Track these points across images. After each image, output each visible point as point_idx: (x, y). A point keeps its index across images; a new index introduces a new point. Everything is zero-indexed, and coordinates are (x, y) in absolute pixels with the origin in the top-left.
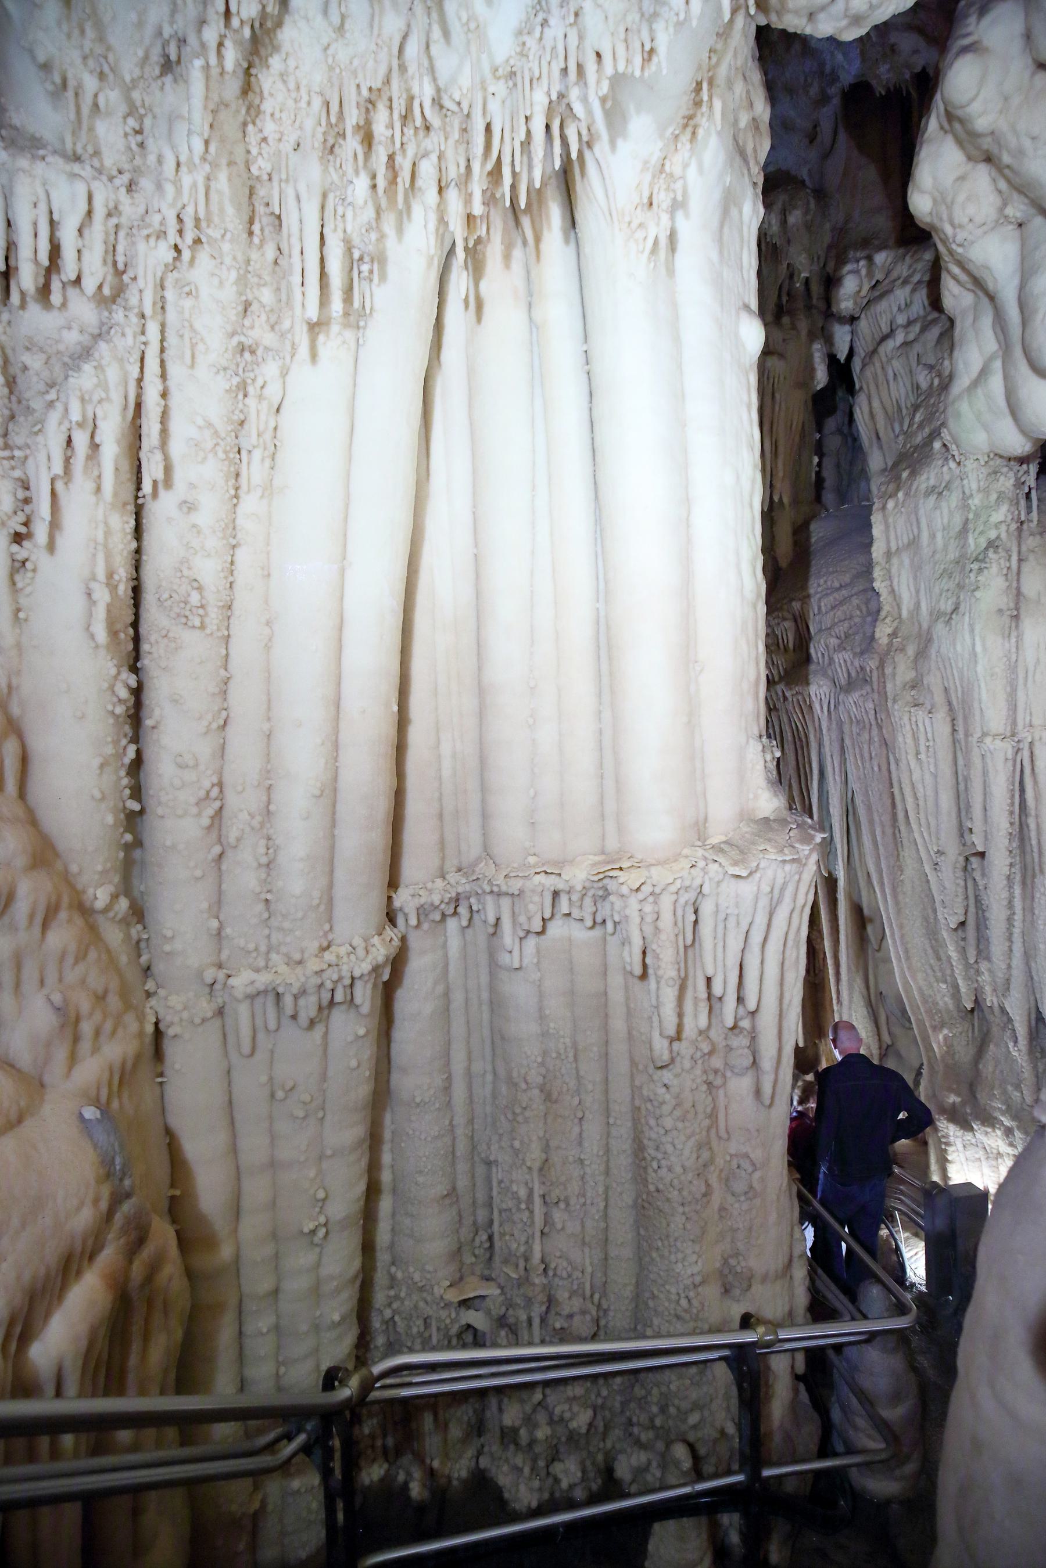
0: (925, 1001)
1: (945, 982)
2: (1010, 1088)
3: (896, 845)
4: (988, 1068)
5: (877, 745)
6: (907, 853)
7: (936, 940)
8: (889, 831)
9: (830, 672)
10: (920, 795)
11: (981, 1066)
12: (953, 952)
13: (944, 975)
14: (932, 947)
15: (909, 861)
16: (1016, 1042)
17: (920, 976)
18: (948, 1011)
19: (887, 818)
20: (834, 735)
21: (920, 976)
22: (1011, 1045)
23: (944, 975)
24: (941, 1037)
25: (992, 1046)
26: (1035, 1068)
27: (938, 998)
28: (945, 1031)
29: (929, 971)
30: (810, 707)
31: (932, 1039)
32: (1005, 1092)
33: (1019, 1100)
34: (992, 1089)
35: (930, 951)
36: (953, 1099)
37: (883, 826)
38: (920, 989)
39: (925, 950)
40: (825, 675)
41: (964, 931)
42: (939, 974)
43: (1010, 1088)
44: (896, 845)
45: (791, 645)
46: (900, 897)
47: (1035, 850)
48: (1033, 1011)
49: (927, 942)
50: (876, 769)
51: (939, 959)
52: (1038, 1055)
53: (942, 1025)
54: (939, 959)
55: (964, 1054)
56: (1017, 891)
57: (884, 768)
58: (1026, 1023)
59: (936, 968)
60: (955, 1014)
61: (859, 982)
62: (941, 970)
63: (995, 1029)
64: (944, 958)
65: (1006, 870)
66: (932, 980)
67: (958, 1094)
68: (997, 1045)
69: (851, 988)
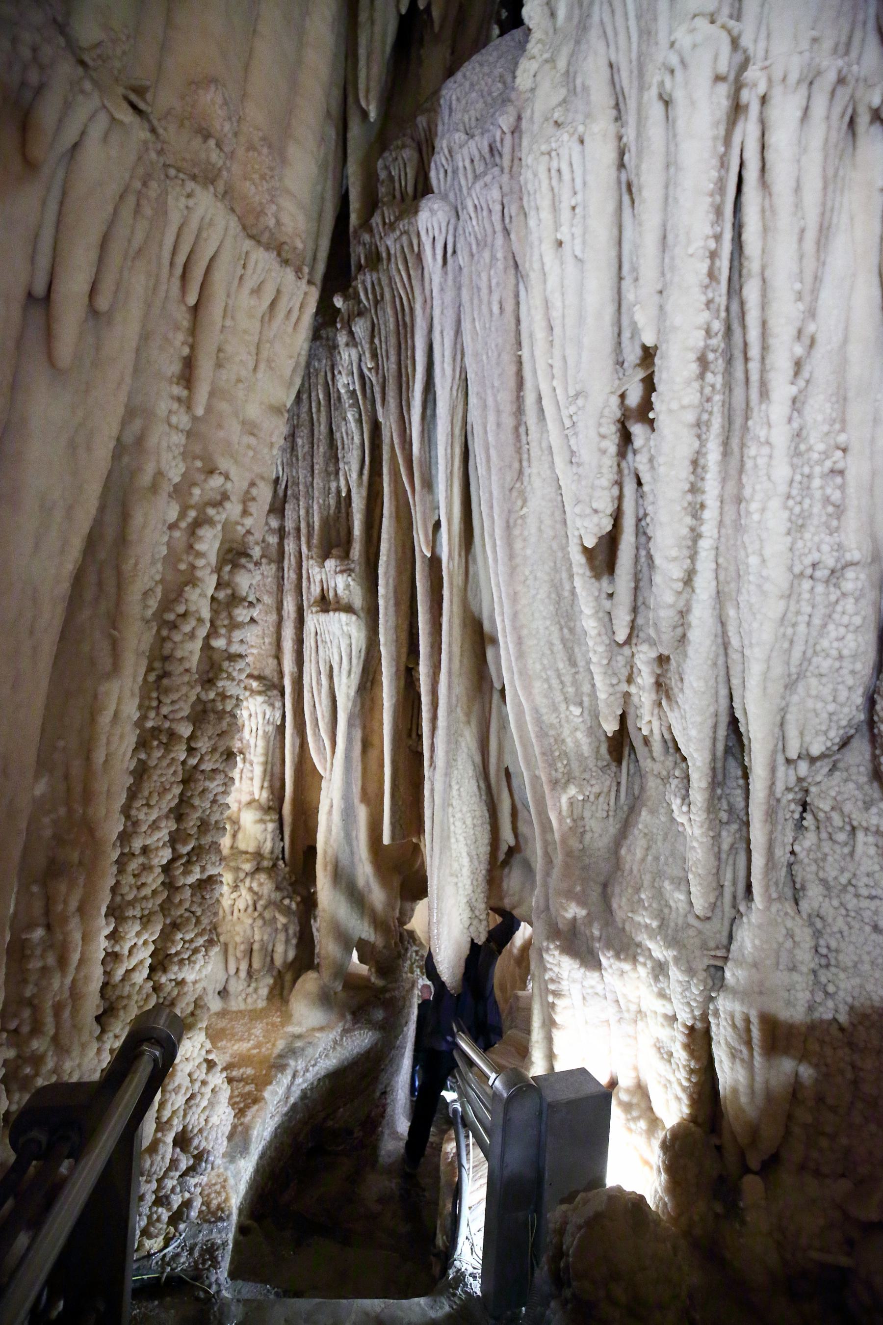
0: (542, 734)
1: (581, 704)
2: (667, 886)
3: (519, 451)
4: (634, 852)
5: (500, 265)
6: (536, 472)
7: (572, 630)
8: (509, 421)
9: (451, 196)
10: (556, 314)
11: (623, 852)
12: (589, 624)
13: (578, 693)
14: (563, 641)
15: (537, 483)
16: (685, 797)
17: (538, 686)
18: (581, 758)
19: (506, 397)
20: (450, 295)
21: (538, 686)
22: (676, 803)
23: (578, 693)
24: (564, 800)
25: (644, 813)
26: (716, 838)
27: (566, 732)
28: (572, 791)
29: (555, 682)
30: (419, 257)
31: (549, 803)
32: (659, 894)
33: (682, 906)
34: (638, 890)
35: (558, 646)
36: (573, 911)
37: (498, 412)
38: (536, 710)
39: (551, 644)
40: (445, 197)
41: (612, 581)
42: (571, 690)
43: (667, 886)
44: (519, 451)
45: (410, 190)
46: (518, 545)
47: (754, 352)
48: (724, 720)
49: (555, 629)
50: (496, 309)
51: (573, 663)
52: (724, 816)
53: (569, 779)
54: (573, 663)
55: (599, 832)
56: (713, 456)
57: (509, 306)
58: (708, 743)
59: (568, 679)
60: (591, 763)
61: (469, 740)
62: (575, 682)
63: (652, 783)
64: (581, 664)
65: (698, 339)
66: (559, 698)
67: (582, 903)
68: (652, 812)
69: (453, 739)
